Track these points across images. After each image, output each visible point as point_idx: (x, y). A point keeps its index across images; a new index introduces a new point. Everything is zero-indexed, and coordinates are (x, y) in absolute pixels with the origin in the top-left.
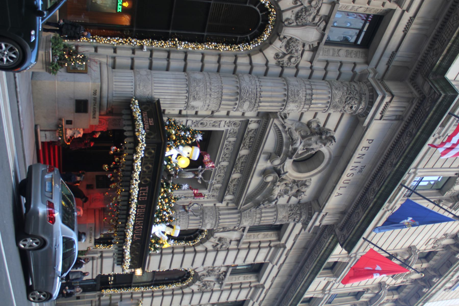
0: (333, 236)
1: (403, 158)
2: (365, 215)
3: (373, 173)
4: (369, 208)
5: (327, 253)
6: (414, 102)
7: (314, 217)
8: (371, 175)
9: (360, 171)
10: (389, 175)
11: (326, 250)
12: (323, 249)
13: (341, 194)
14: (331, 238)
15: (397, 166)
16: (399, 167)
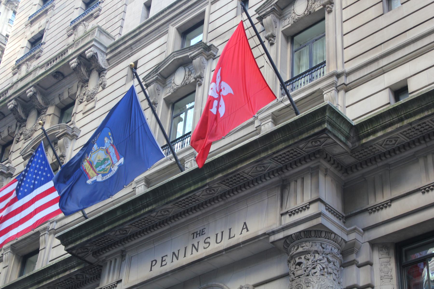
0: (364, 141)
1: (138, 214)
2: (239, 166)
3: (199, 213)
4: (225, 173)
5: (415, 108)
6: (104, 258)
7: (281, 235)
8: (204, 211)
9: (202, 233)
10: (167, 203)
11: (407, 117)
12: (411, 124)
13: (245, 223)
14: (371, 138)
15: (150, 208)
16: (151, 204)
